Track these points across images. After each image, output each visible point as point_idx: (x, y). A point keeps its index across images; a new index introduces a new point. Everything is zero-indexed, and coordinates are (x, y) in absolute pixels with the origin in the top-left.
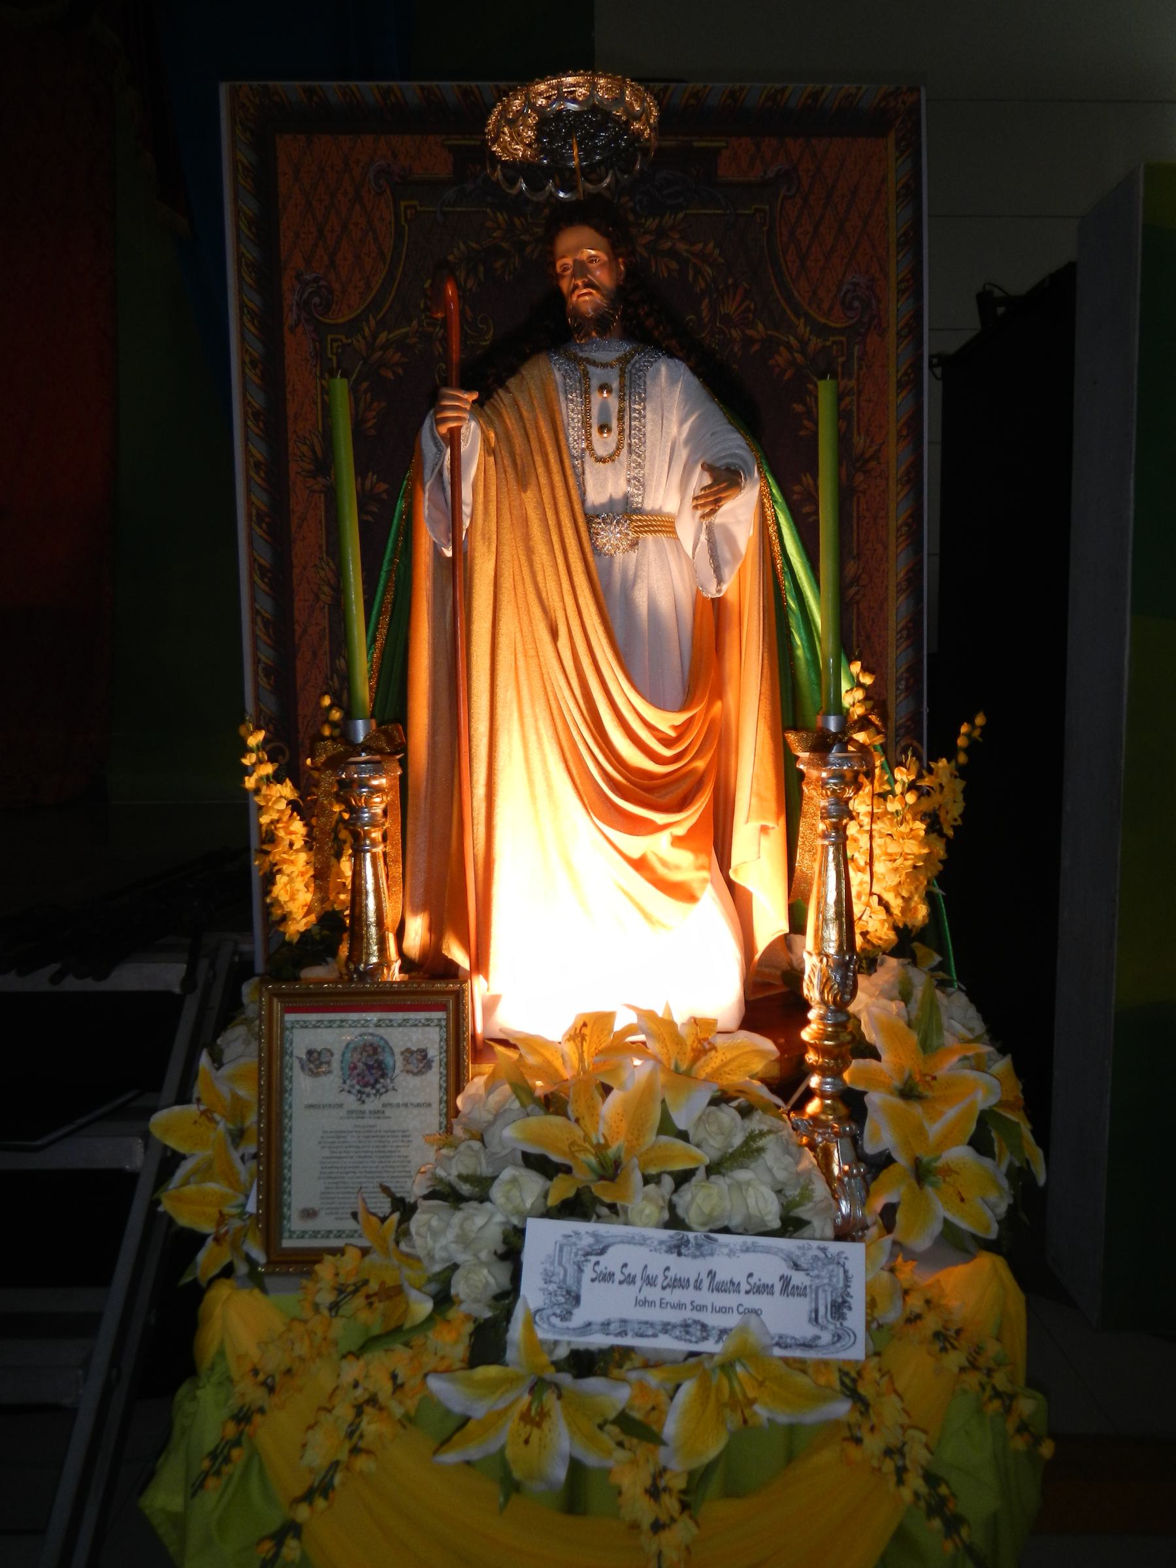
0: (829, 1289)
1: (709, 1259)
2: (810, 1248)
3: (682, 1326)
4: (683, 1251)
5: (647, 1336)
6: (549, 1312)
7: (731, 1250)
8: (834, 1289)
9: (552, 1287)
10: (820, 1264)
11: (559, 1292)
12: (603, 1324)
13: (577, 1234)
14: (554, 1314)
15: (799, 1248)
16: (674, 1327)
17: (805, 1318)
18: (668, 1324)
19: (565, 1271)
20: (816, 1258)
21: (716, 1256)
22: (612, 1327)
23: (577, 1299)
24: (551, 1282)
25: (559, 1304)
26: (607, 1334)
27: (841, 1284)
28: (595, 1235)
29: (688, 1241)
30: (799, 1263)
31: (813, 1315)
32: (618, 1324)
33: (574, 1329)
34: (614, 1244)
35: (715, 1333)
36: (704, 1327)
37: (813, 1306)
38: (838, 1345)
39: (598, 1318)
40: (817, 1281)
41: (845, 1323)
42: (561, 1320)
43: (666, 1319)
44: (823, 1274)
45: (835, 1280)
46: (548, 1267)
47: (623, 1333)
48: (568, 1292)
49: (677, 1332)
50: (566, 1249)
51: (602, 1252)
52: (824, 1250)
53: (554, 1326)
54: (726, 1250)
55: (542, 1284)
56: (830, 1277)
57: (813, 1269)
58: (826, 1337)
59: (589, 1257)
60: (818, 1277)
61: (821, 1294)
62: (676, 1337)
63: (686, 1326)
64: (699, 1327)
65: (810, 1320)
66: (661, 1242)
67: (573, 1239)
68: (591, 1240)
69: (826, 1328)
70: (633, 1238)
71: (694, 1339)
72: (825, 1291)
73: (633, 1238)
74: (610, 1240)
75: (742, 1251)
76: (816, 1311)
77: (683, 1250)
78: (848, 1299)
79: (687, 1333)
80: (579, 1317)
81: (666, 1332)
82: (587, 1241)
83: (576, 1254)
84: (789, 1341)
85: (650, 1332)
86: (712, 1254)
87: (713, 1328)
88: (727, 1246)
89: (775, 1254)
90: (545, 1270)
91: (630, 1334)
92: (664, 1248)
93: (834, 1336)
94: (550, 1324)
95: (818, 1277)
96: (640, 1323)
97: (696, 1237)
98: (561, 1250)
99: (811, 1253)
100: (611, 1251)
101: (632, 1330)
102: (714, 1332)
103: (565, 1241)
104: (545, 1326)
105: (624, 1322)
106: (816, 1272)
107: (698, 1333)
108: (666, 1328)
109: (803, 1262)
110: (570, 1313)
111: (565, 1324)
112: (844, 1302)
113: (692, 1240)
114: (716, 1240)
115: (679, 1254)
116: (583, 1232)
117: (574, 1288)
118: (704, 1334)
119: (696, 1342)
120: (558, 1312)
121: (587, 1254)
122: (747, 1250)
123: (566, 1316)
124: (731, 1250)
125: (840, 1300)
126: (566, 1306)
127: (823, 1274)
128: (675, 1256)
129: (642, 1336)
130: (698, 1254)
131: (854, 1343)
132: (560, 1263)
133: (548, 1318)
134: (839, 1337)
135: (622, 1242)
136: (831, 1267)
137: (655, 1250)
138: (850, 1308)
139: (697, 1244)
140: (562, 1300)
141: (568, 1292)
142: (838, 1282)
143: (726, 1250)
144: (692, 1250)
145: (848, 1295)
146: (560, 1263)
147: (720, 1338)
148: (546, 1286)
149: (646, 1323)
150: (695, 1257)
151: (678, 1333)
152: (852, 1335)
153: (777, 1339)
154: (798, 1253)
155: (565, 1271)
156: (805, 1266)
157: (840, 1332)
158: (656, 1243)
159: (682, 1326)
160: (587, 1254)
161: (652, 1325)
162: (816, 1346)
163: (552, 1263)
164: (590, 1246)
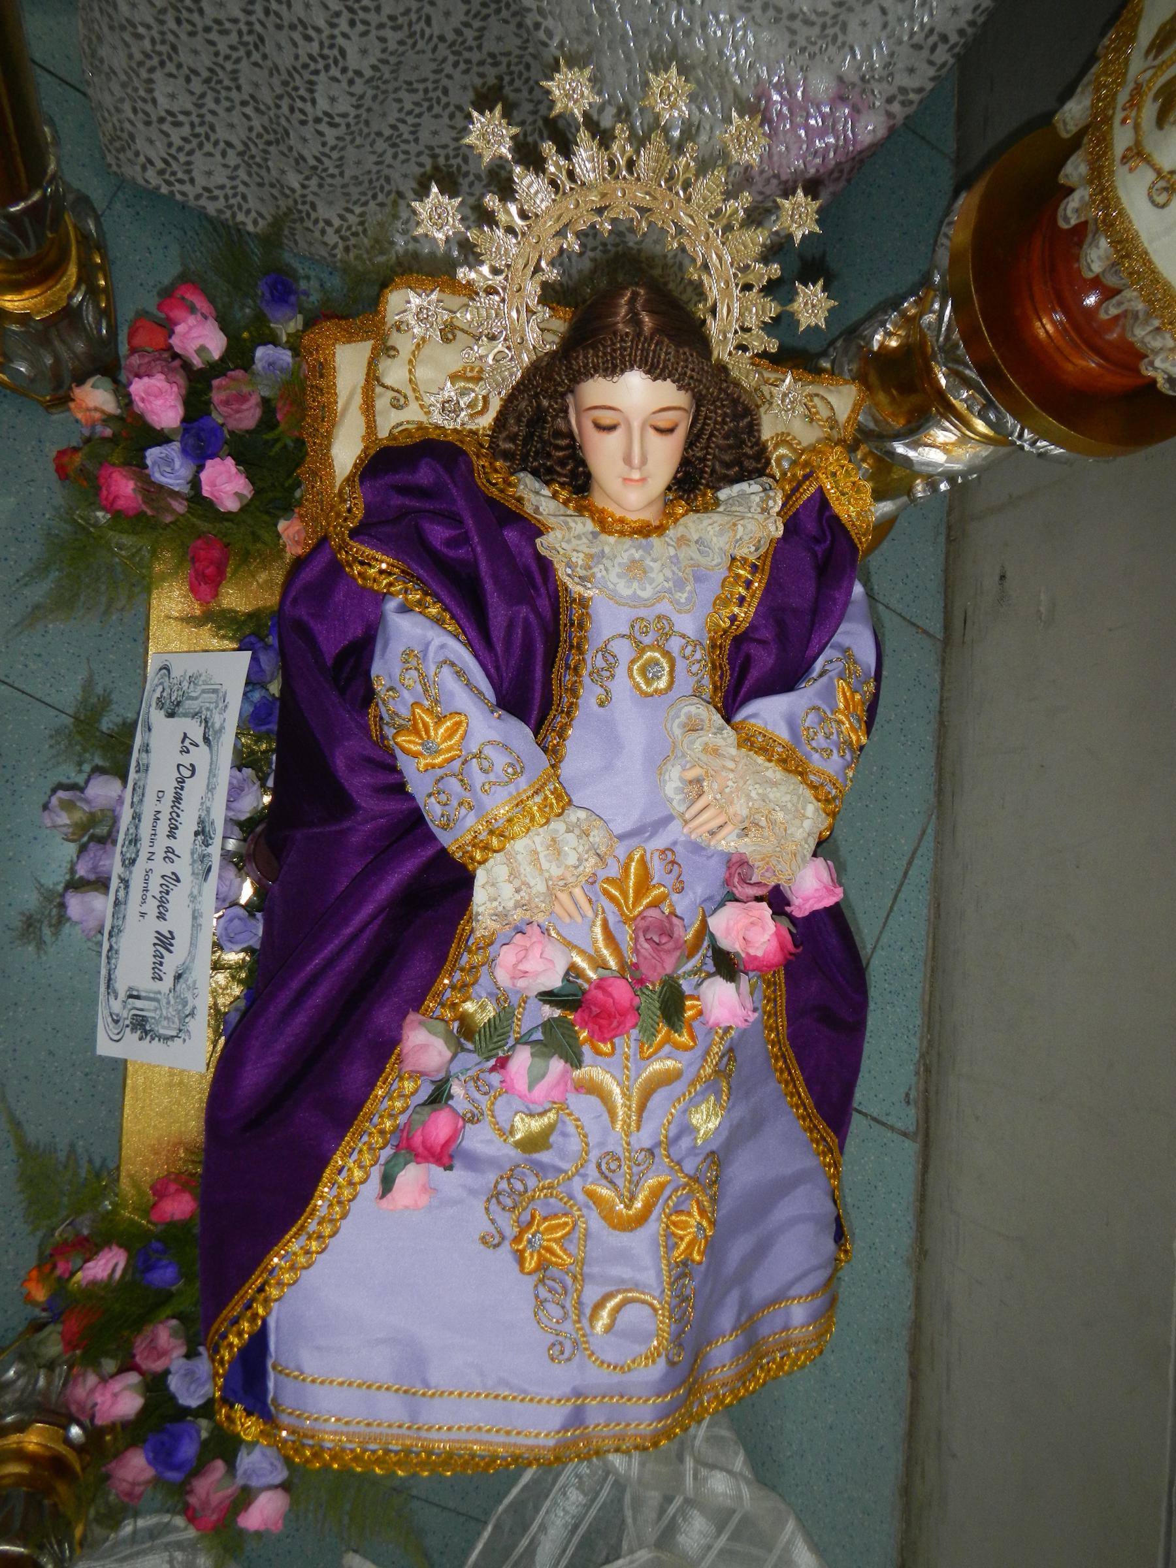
0: (156, 1015)
1: (190, 869)
2: (195, 996)
7: (195, 897)
8: (158, 1022)
10: (180, 1007)
15: (195, 982)
16: (137, 827)
17: (132, 985)
19: (196, 698)
20: (185, 1003)
21: (192, 878)
22: (144, 755)
27: (162, 1031)
28: (222, 728)
29: (207, 846)
30: (181, 980)
31: (135, 993)
32: (145, 762)
35: (126, 875)
37: (143, 994)
38: (110, 1019)
40: (164, 1002)
41: (128, 1030)
43: (143, 817)
44: (171, 1012)
45: (165, 1023)
50: (214, 696)
51: (206, 740)
52: (192, 1014)
54: (195, 892)
56: (167, 1018)
57: (175, 998)
58: (116, 1006)
60: (168, 1003)
61: (154, 1004)
63: (135, 841)
65: (131, 989)
66: (208, 810)
67: (221, 705)
68: (217, 726)
69: (124, 1007)
70: (214, 776)
71: (125, 849)
72: (155, 1010)
73: (214, 776)
75: (194, 911)
76: (138, 997)
77: (200, 838)
78: (148, 1038)
79: (130, 842)
81: (133, 818)
82: (217, 720)
83: (208, 709)
86: (193, 873)
88: (200, 893)
89: (190, 952)
91: (136, 776)
92: (203, 814)
93: (117, 1015)
95: (168, 1003)
97: (209, 855)
99: (189, 996)
103: (221, 695)
106: (172, 1002)
107: (128, 855)
108: (137, 817)
109: (181, 986)
112: (146, 1033)
113: (210, 850)
114: (205, 880)
115: (196, 834)
121: (206, 722)
122: (194, 918)
124: (195, 897)
125: (148, 1028)
127: (171, 1009)
128: (196, 828)
129: (134, 789)
130: (196, 856)
134: (116, 1022)
135: (211, 764)
136: (176, 1020)
137: (202, 804)
138: (140, 1039)
139: (204, 856)
142: (164, 1027)
143: (195, 892)
144: (199, 850)
145: (152, 1039)
149: (143, 795)
150: (192, 854)
151: (131, 831)
152: (117, 1038)
154: (190, 981)
155: (196, 698)
156: (178, 988)
157: (121, 1023)
158: (208, 804)
160: (206, 722)
161: (141, 801)
164: (213, 724)
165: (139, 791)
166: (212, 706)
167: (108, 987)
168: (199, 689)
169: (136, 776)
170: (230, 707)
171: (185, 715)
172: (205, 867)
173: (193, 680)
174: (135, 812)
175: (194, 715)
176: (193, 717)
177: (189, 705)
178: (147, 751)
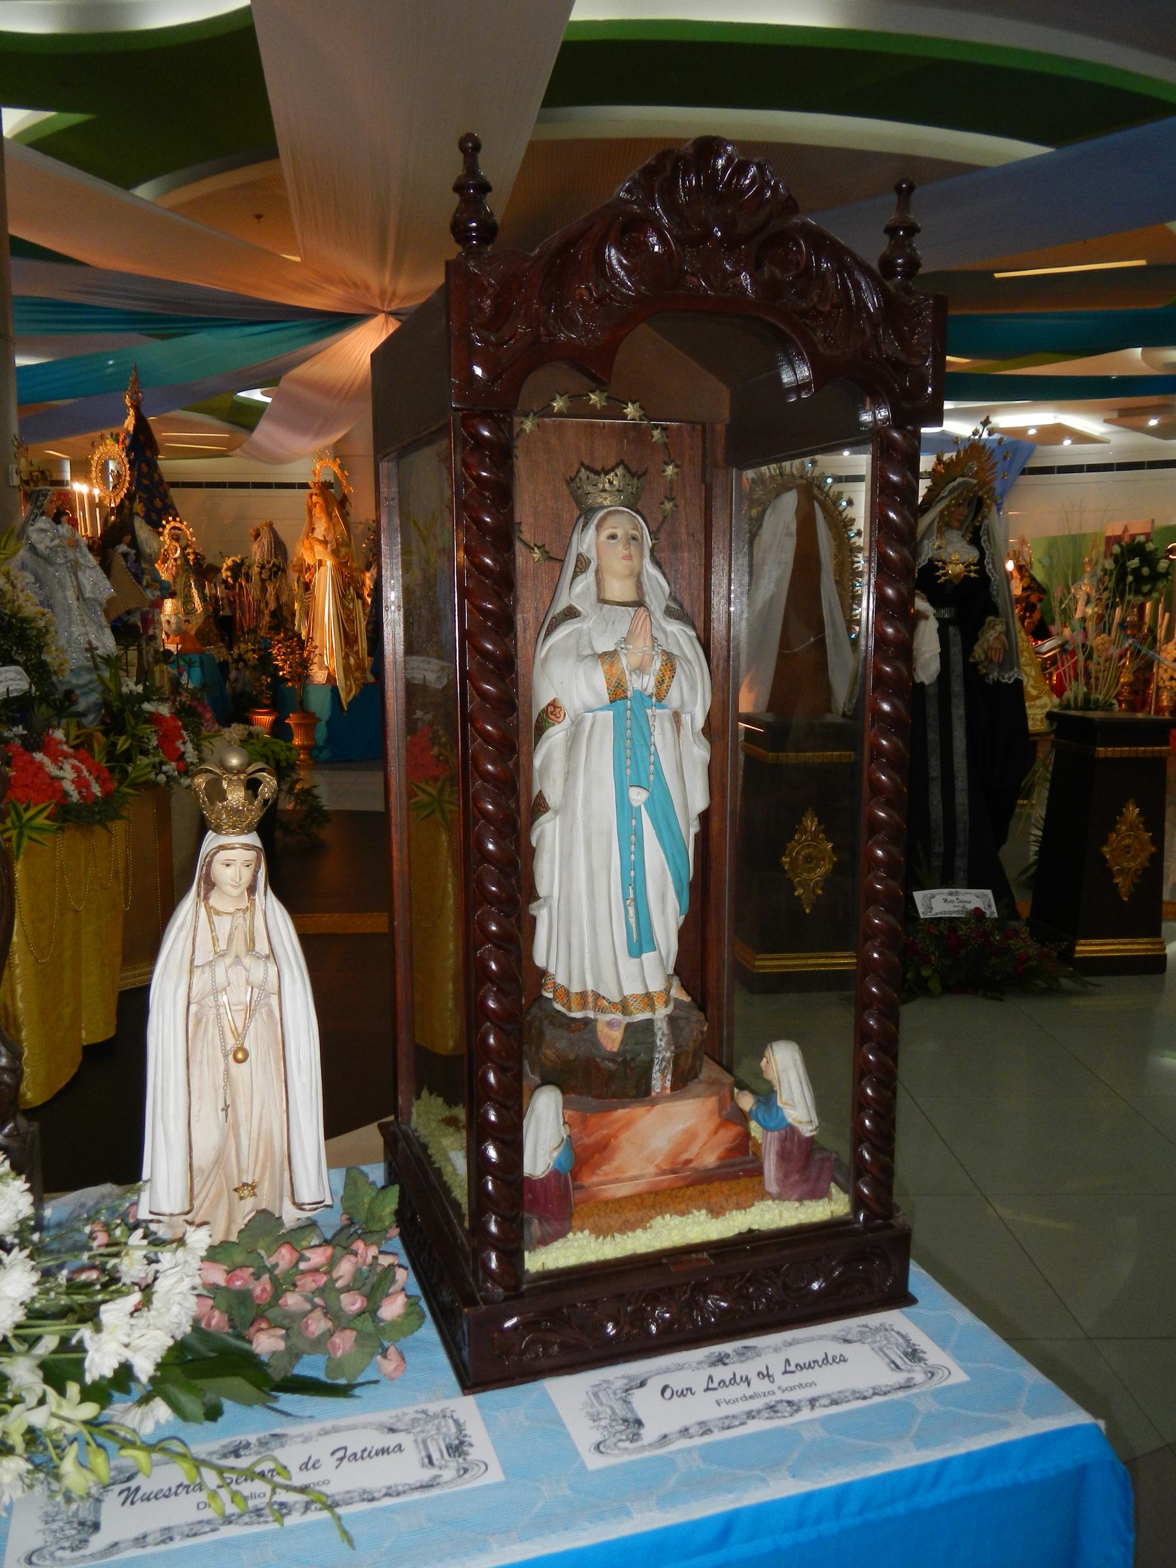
3: (766, 1409)
4: (727, 1361)
5: (733, 1427)
6: (614, 1440)
9: (603, 1423)
11: (614, 1424)
12: (681, 1432)
13: (604, 1381)
14: (620, 1440)
16: (759, 1412)
18: (751, 1411)
22: (692, 1431)
23: (639, 1423)
24: (600, 1419)
25: (621, 1432)
26: (691, 1437)
28: (623, 1377)
32: (697, 1428)
33: (650, 1445)
34: (650, 1377)
36: (790, 1403)
39: (673, 1427)
42: (631, 1442)
46: (590, 1410)
47: (709, 1431)
48: (625, 1421)
49: (765, 1414)
50: (601, 1394)
53: (626, 1449)
55: (591, 1423)
59: (631, 1392)
62: (767, 1418)
64: (785, 1404)
68: (625, 1381)
71: (786, 1414)
74: (645, 1376)
79: (776, 1412)
80: (649, 1434)
81: (753, 1418)
83: (615, 1394)
84: (884, 1388)
85: (737, 1423)
87: (800, 1401)
90: (588, 1413)
94: (620, 1449)
96: (720, 1419)
98: (596, 1395)
100: (649, 1382)
101: (717, 1426)
102: (802, 1403)
103: (596, 1389)
104: (616, 1452)
105: (701, 1423)
107: (788, 1409)
108: (750, 1415)
110: (638, 1434)
111: (638, 1444)
115: (725, 1364)
116: (611, 1378)
117: (629, 1416)
118: (795, 1408)
119: (791, 1415)
120: (624, 1437)
123: (635, 1437)
126: (629, 1431)
130: (743, 1359)
131: (950, 1373)
132: (601, 1404)
133: (615, 1445)
140: (623, 1428)
141: (625, 1421)
146: (601, 1404)
147: (813, 1407)
148: (596, 1424)
151: (766, 1415)
153: (871, 1391)
159: (766, 1409)
160: (627, 1390)
161: (734, 1417)
162: (915, 1385)
163: (592, 1406)
165: (727, 1422)
166: (610, 1392)
167: (910, 1387)
168: (601, 1409)
169: (716, 1430)
170: (602, 1378)
171: (632, 1410)
172: (745, 1351)
173: (595, 1418)
174: (748, 1418)
175: (626, 1402)
176: (629, 1402)
177: (621, 1411)
178: (687, 1430)
